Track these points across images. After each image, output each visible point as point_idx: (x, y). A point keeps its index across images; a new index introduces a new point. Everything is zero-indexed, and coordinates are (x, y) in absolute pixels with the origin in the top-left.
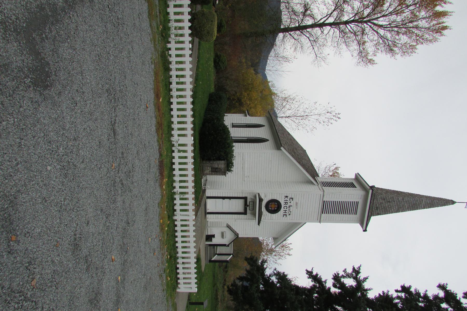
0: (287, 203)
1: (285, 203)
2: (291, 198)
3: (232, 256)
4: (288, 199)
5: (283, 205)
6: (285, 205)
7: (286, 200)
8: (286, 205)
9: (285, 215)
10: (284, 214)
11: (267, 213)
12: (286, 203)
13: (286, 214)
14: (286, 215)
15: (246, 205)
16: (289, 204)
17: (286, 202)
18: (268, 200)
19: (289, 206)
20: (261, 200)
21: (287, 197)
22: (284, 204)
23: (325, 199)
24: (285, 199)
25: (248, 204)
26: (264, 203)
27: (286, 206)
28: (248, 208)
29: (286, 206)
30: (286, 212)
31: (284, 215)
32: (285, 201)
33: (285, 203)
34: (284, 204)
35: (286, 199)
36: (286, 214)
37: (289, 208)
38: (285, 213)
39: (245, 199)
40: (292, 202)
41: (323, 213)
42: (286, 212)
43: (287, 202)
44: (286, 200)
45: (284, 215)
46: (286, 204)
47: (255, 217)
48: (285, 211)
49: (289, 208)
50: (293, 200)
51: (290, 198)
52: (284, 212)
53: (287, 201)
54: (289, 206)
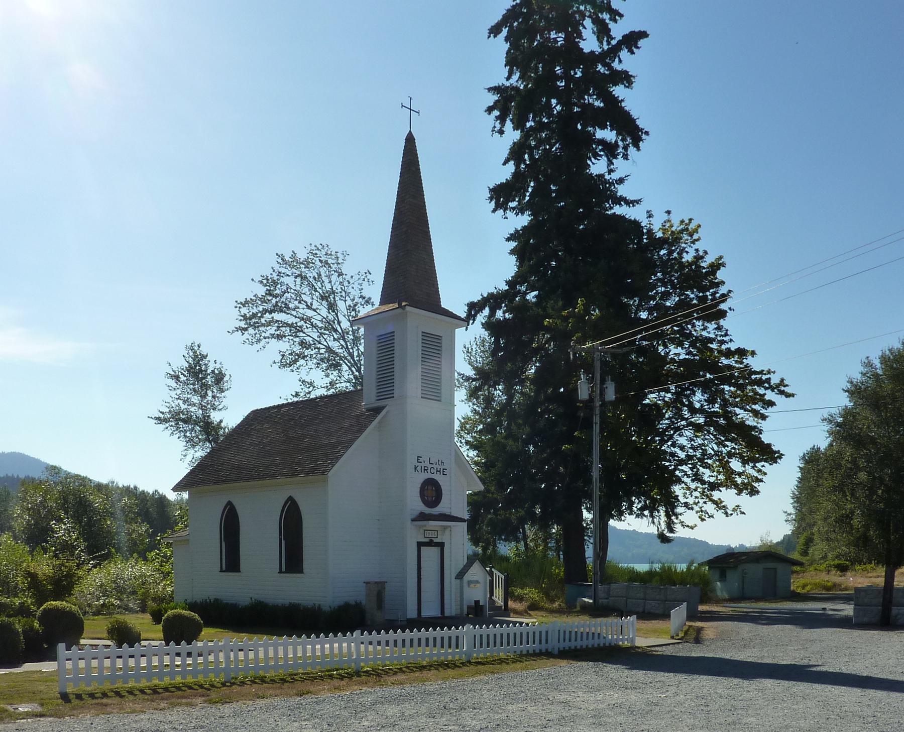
0: (426, 468)
2: (418, 459)
3: (493, 570)
4: (419, 464)
6: (429, 471)
8: (429, 469)
9: (443, 472)
10: (442, 473)
11: (441, 505)
15: (430, 543)
16: (427, 464)
17: (425, 470)
18: (421, 504)
20: (422, 517)
21: (415, 468)
24: (420, 471)
25: (427, 540)
26: (427, 510)
28: (435, 540)
30: (438, 470)
31: (443, 474)
32: (423, 471)
35: (419, 468)
38: (440, 471)
39: (420, 545)
42: (438, 470)
45: (443, 474)
46: (427, 470)
47: (450, 526)
48: (437, 471)
53: (423, 468)
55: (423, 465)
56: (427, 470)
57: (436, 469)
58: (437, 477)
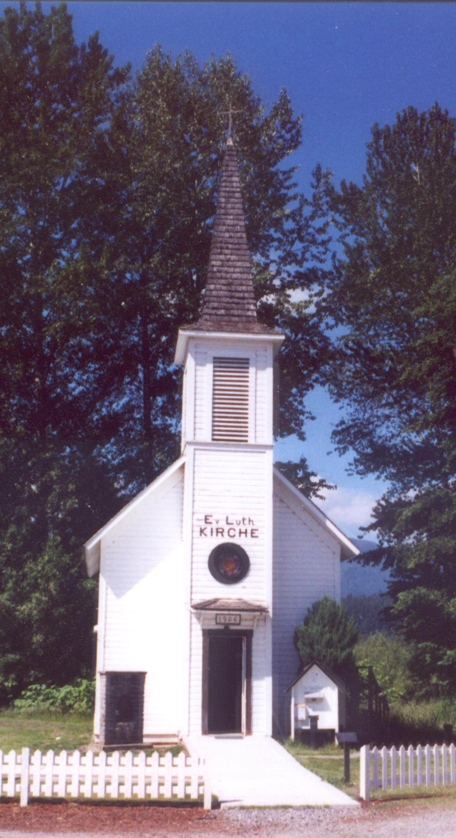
1: (220, 535)
2: (206, 519)
4: (209, 527)
5: (225, 539)
6: (226, 534)
7: (212, 532)
9: (252, 533)
10: (249, 535)
12: (220, 531)
13: (249, 532)
14: (252, 530)
16: (222, 524)
17: (217, 532)
19: (227, 523)
21: (202, 531)
22: (223, 536)
23: (209, 439)
27: (229, 532)
29: (229, 532)
31: (252, 536)
32: (214, 533)
33: (220, 535)
34: (223, 536)
35: (208, 532)
36: (249, 532)
37: (232, 524)
38: (246, 532)
40: (215, 517)
41: (246, 441)
42: (243, 530)
43: (217, 529)
44: (212, 532)
48: (240, 533)
49: (232, 524)
50: (211, 516)
51: (206, 523)
52: (243, 535)
53: (215, 531)
54: (227, 523)
55: (214, 526)
56: (222, 533)
57: (238, 531)
58: (238, 541)
